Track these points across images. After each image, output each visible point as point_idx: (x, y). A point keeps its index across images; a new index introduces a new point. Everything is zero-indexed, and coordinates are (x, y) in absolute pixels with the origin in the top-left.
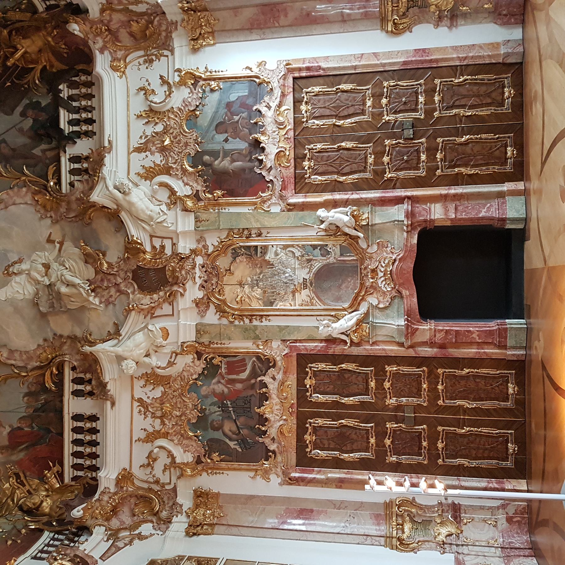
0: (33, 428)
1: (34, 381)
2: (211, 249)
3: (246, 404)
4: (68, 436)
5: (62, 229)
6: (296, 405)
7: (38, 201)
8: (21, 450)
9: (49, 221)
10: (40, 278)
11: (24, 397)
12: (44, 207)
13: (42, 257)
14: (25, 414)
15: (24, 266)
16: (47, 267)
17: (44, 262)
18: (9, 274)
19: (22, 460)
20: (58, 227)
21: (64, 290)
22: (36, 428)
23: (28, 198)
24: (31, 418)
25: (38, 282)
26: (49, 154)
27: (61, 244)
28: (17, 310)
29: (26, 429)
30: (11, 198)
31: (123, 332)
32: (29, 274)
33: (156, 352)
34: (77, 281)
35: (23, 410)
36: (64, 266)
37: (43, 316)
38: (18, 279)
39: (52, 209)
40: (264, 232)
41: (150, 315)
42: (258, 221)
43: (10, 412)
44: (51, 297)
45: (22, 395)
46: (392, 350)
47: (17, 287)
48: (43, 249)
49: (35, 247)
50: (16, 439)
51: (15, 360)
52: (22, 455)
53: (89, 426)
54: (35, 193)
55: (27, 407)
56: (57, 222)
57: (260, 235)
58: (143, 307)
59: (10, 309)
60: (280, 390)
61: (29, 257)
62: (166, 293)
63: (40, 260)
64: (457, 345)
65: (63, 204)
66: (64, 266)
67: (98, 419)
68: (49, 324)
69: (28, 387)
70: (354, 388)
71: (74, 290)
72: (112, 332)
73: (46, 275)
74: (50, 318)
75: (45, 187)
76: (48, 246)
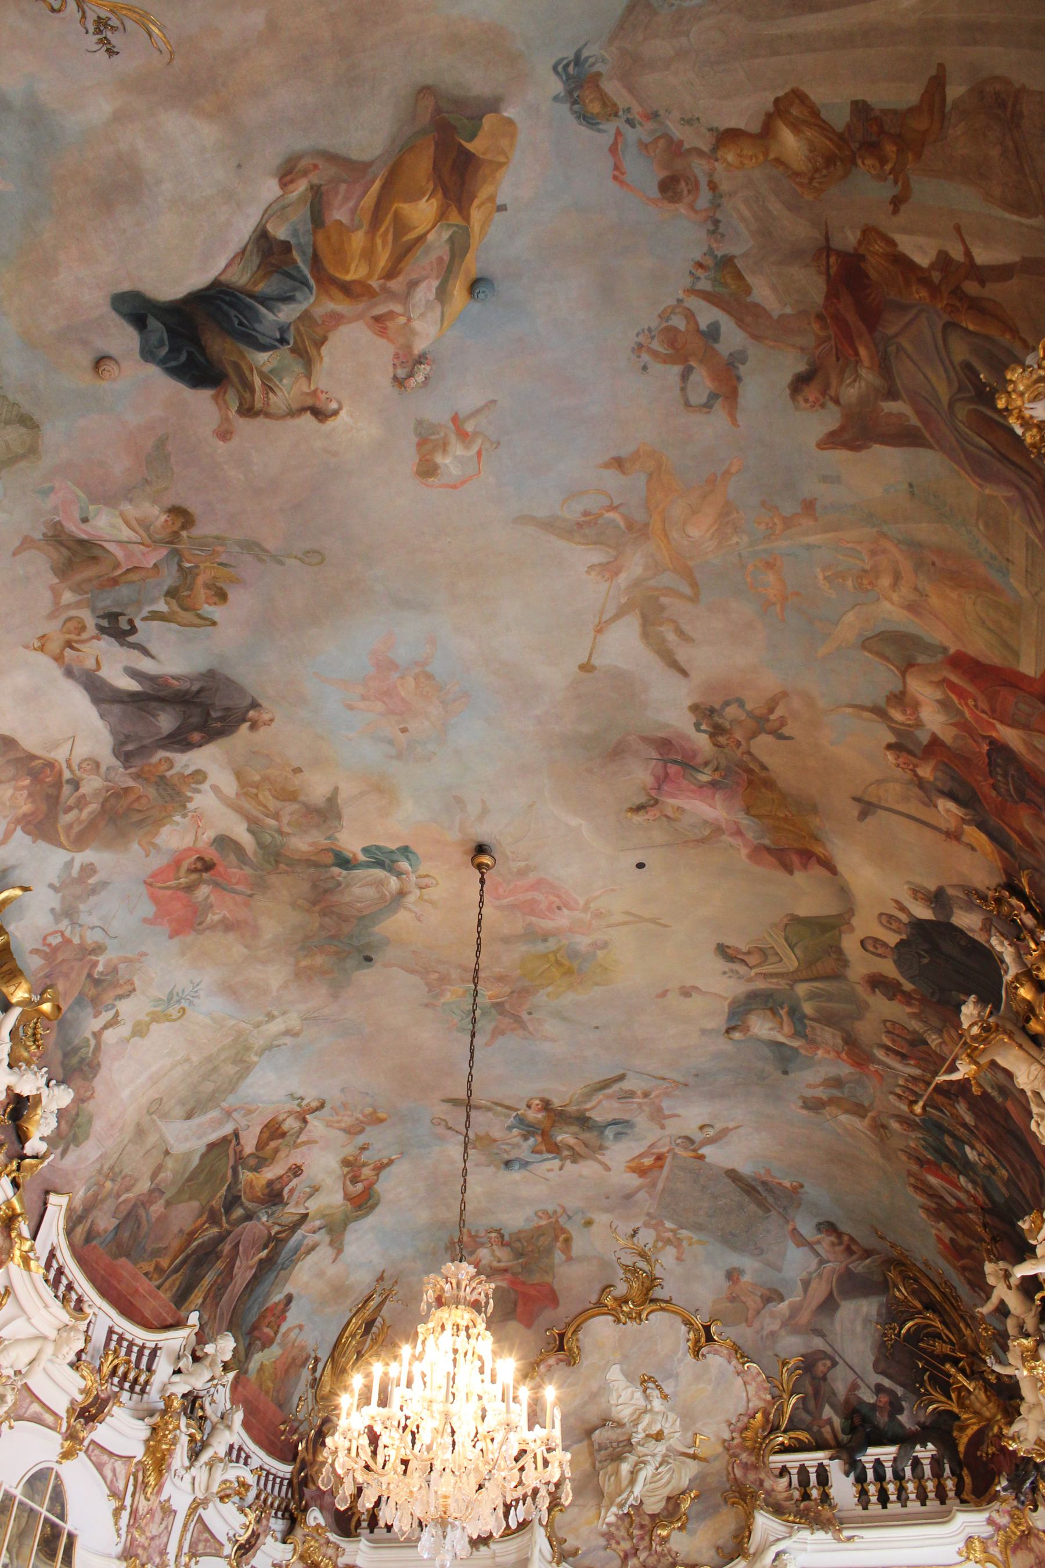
5: (717, 1457)
7: (754, 1417)
9: (727, 1436)
10: (640, 1427)
12: (746, 1428)
13: (671, 1426)
15: (657, 1404)
16: (659, 1437)
17: (666, 1432)
18: (646, 1382)
20: (720, 1449)
21: (625, 1468)
23: (756, 1403)
25: (636, 1423)
26: (826, 1430)
27: (694, 1457)
28: (594, 1396)
30: (754, 1379)
32: (645, 1412)
34: (638, 1489)
36: (661, 1465)
37: (589, 1433)
38: (638, 1395)
39: (744, 1439)
44: (615, 1445)
47: (625, 1395)
48: (685, 1428)
49: (688, 1418)
54: (766, 1414)
56: (727, 1449)
59: (594, 1386)
61: (672, 1409)
63: (667, 1425)
65: (753, 1459)
66: (661, 1465)
68: (576, 1442)
71: (625, 1482)
73: (648, 1436)
74: (585, 1443)
75: (775, 1429)
76: (690, 1434)
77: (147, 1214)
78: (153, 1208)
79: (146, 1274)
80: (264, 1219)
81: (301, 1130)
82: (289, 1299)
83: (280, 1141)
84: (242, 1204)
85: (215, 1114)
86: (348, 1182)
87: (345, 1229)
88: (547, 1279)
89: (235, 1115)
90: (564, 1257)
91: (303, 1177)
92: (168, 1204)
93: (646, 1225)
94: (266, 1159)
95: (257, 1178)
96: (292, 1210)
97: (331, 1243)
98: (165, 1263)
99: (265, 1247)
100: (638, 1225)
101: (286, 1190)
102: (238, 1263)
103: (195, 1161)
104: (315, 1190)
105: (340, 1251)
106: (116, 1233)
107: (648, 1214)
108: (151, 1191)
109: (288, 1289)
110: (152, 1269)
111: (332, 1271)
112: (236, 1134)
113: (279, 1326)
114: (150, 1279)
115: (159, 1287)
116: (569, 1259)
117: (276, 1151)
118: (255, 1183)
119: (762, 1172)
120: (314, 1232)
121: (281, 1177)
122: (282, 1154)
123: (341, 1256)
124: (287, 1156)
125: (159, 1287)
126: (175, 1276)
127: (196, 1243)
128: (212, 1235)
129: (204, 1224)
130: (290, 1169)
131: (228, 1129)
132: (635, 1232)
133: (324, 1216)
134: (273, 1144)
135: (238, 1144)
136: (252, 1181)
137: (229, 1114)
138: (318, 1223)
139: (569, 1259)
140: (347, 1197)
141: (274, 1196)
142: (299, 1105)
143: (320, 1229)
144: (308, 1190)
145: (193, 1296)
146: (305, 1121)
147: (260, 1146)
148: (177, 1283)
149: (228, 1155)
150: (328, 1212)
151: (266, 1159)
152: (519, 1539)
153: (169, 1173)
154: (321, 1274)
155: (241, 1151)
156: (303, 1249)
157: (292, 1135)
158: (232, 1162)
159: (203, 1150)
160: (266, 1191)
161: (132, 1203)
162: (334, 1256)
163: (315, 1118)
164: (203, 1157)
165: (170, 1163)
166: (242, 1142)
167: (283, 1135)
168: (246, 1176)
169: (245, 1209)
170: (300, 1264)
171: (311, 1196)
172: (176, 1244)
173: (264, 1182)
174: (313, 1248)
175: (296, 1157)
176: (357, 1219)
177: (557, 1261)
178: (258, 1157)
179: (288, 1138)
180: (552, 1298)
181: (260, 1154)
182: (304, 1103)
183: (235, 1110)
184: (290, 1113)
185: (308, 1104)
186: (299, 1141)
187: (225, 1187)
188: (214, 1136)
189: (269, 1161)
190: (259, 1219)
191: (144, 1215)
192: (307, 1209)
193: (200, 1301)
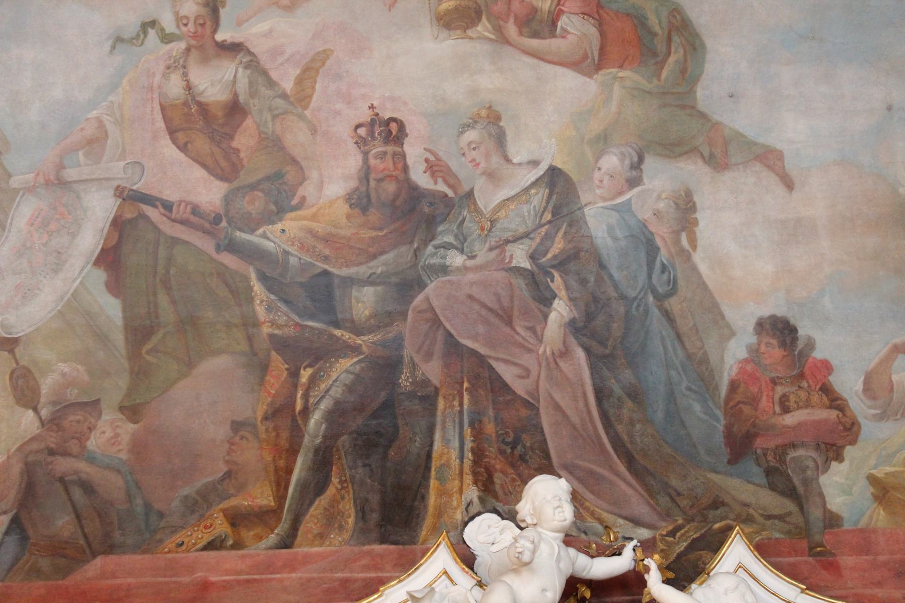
77: (91, 460)
78: (93, 443)
79: (210, 546)
80: (456, 259)
81: (254, 65)
82: (781, 330)
83: (249, 122)
84: (350, 282)
85: (25, 212)
86: (535, 43)
87: (703, 116)
89: (71, 174)
91: (416, 127)
92: (131, 411)
94: (278, 176)
95: (314, 217)
96: (505, 194)
97: (718, 161)
98: (261, 496)
99: (546, 300)
101: (421, 178)
102: (507, 373)
103: (112, 309)
104: (492, 122)
105: (769, 158)
106: (24, 538)
108: (53, 423)
109: (743, 316)
110: (221, 527)
111: (816, 201)
112: (131, 197)
113: (826, 389)
114: (238, 545)
115: (287, 543)
117: (273, 144)
118: (319, 227)
120: (634, 182)
121: (366, 172)
122: (296, 137)
123: (790, 165)
124: (314, 131)
125: (287, 543)
126: (322, 501)
127: (316, 417)
128: (348, 379)
129: (294, 374)
130: (361, 142)
131: (100, 207)
133: (602, 142)
134: (244, 140)
135: (168, 206)
136: (312, 233)
137: (57, 183)
138: (611, 162)
140: (577, 64)
141: (412, 211)
142: (166, 38)
143: (637, 165)
144: (471, 135)
145: (432, 500)
146: (233, 49)
147: (225, 168)
148: (348, 507)
149: (175, 241)
150: (596, 126)
151: (278, 176)
153: (64, 367)
154: (795, 231)
155: (196, 210)
156: (661, 232)
157: (253, 93)
158: (206, 244)
159: (100, 276)
160: (374, 215)
161: (17, 469)
162: (771, 179)
163: (239, 23)
164: (115, 287)
165: (43, 354)
166: (171, 195)
167: (235, 110)
168: (279, 237)
169: (370, 281)
170: (698, 258)
171: (500, 140)
172: (254, 455)
173: (343, 209)
174: (685, 209)
175: (338, 115)
176: (688, 76)
178: (253, 187)
179: (254, 105)
181: (245, 178)
182: (169, 24)
183: (61, 167)
184: (179, 65)
185: (180, 20)
186: (288, 85)
187: (258, 288)
188: (90, 239)
189: (291, 175)
190: (444, 270)
191: (82, 466)
192: (535, 163)
193: (472, 493)
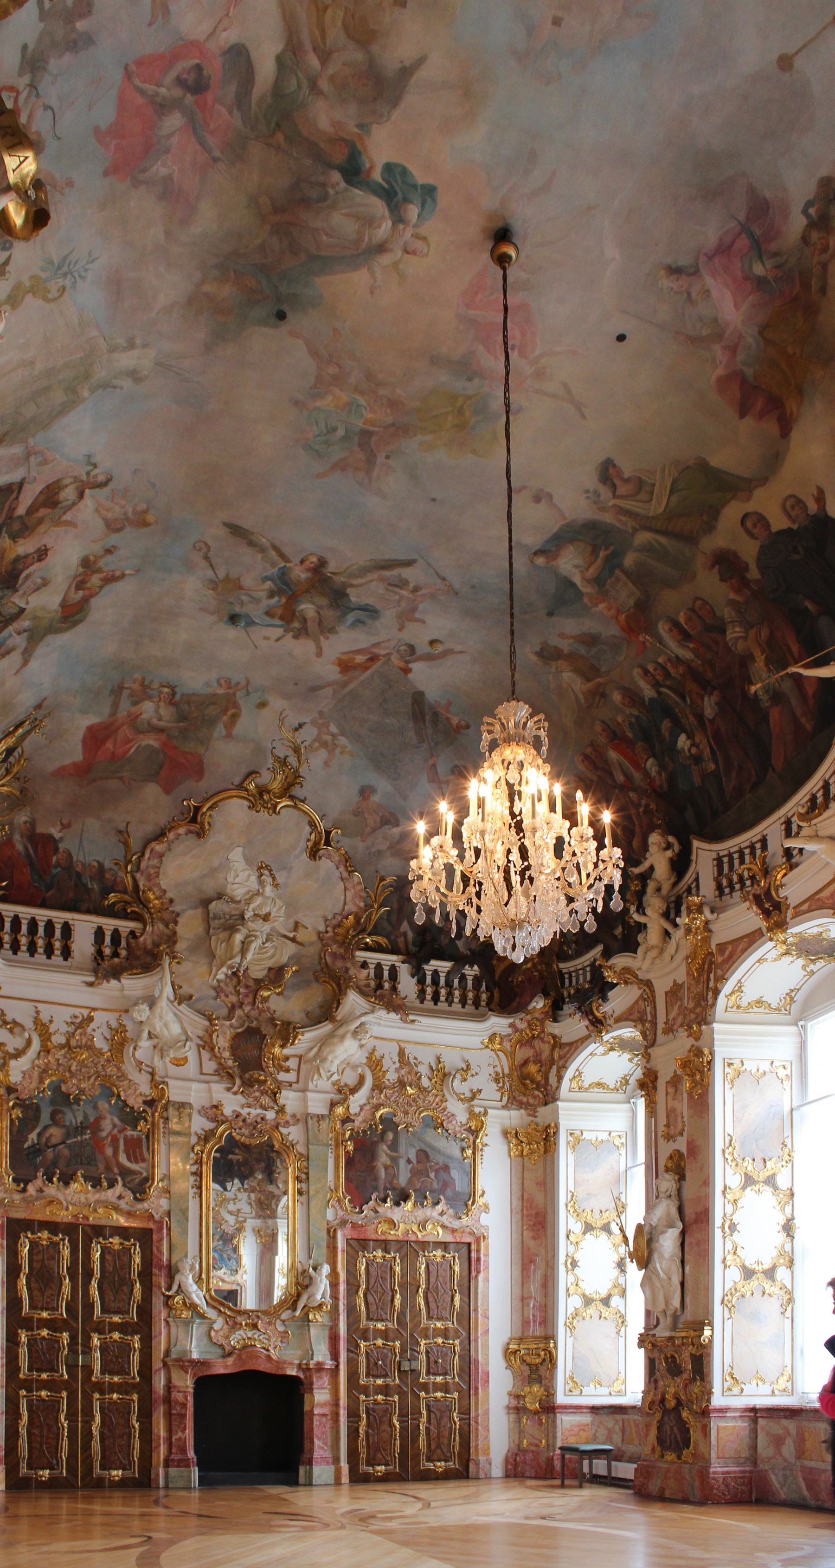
0: (55, 867)
1: (118, 879)
2: (284, 1130)
3: (82, 1159)
4: (43, 915)
6: (86, 1222)
8: (26, 848)
11: (98, 862)
14: (75, 859)
19: (13, 846)
22: (54, 871)
24: (69, 864)
29: (54, 859)
31: (183, 1007)
33: (155, 1047)
35: (81, 858)
40: (304, 1198)
41: (201, 1043)
42: (317, 1192)
43: (81, 842)
45: (101, 860)
46: (160, 1343)
50: (44, 844)
51: (149, 859)
52: (20, 847)
53: (55, 946)
55: (83, 865)
57: (300, 1193)
58: (214, 1036)
60: (106, 1205)
62: (230, 1068)
64: (169, 1415)
67: (66, 959)
69: (111, 869)
70: (110, 1296)
72: (182, 991)
88: (201, 750)
90: (224, 733)
93: (313, 723)
100: (307, 720)
107: (320, 713)
116: (229, 736)
119: (443, 702)
132: (300, 726)
139: (229, 736)
152: (147, 979)
177: (216, 735)
180: (198, 770)
